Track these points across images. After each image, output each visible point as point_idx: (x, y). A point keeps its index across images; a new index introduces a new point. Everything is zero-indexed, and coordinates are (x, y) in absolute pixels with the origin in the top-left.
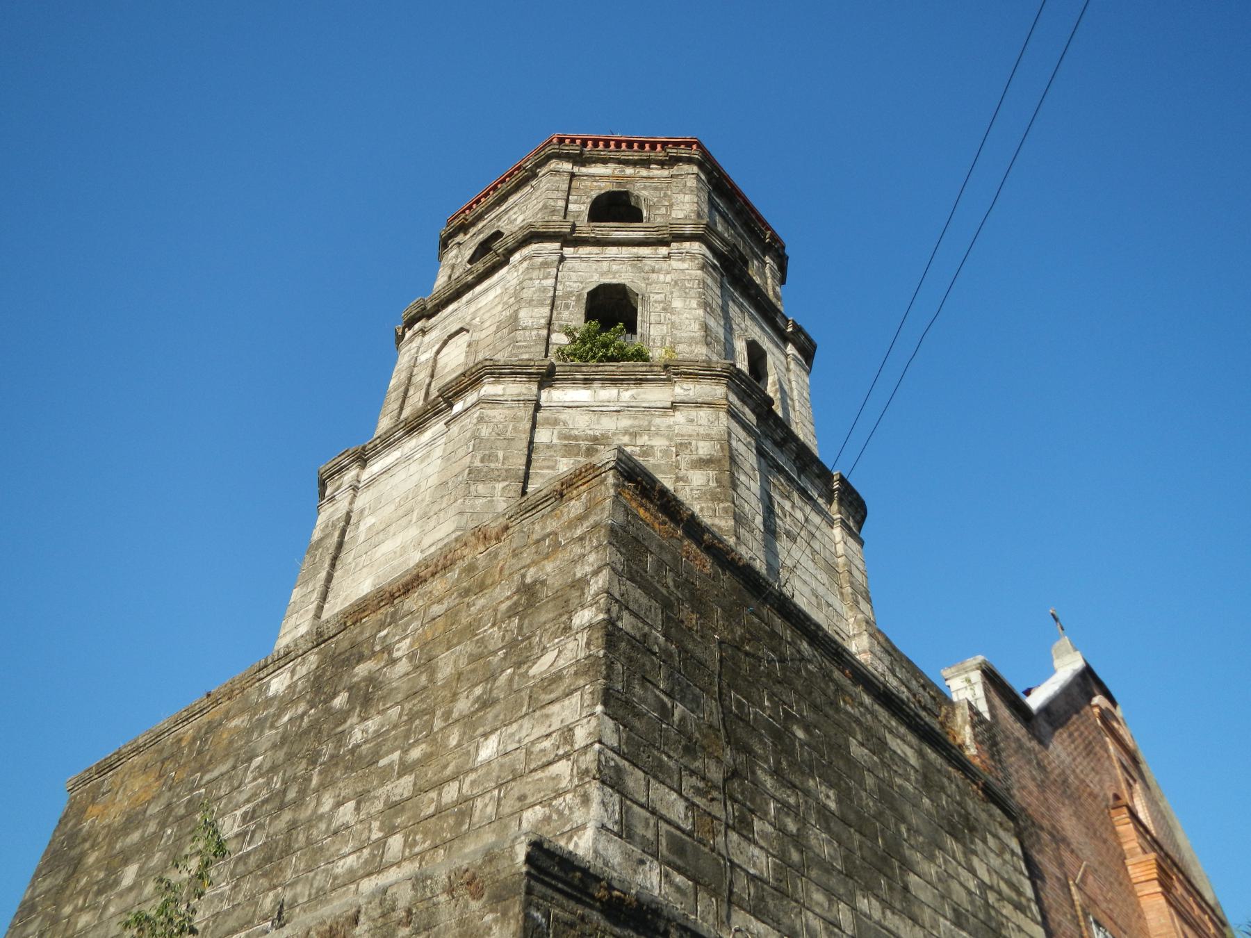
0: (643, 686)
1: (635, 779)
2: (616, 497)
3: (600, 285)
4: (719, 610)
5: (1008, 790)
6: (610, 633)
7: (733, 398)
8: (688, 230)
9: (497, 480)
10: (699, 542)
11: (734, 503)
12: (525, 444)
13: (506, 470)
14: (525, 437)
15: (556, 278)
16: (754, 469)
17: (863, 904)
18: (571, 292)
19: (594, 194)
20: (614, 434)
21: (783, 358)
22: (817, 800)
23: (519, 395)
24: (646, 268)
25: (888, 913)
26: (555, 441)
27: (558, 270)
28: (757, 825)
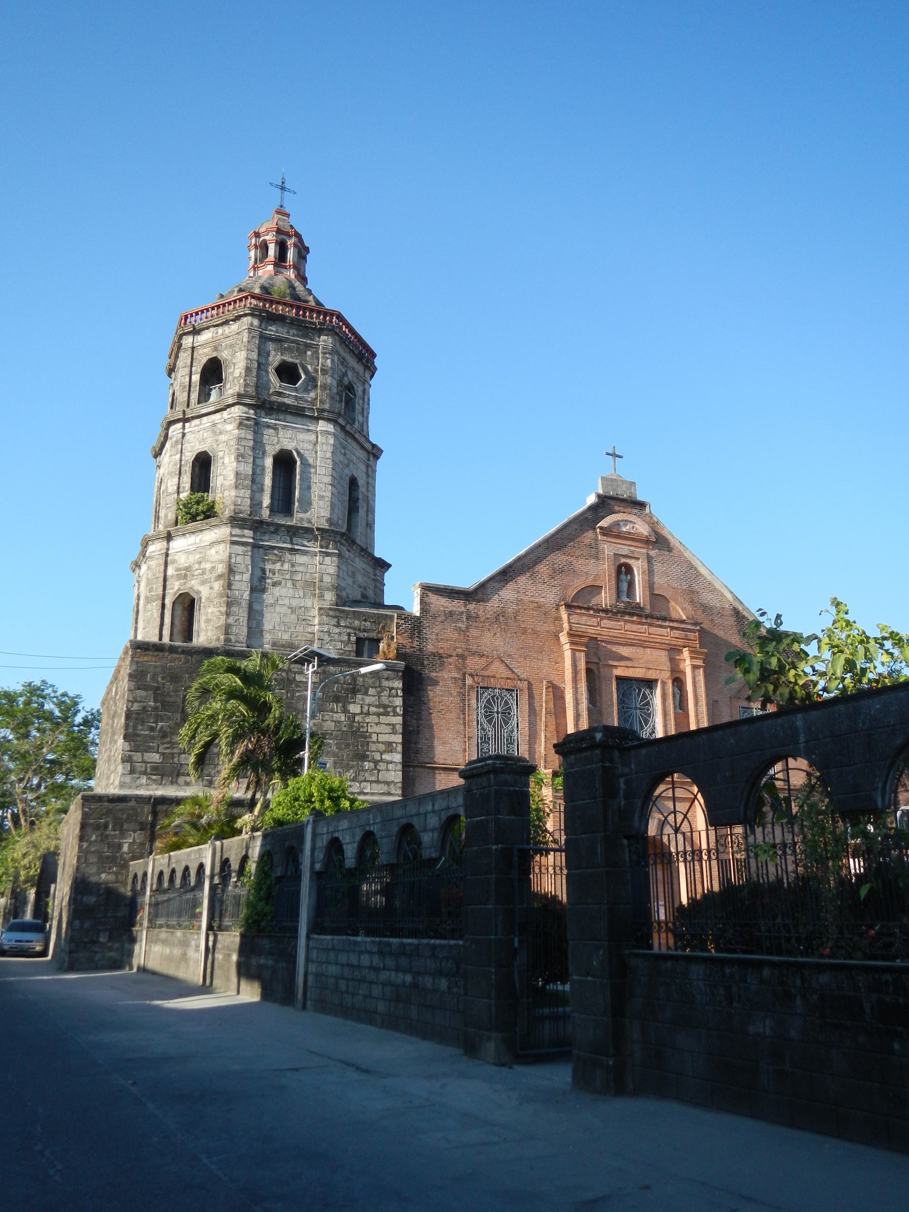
0: (142, 725)
1: (137, 756)
2: (132, 660)
3: (199, 453)
4: (187, 676)
5: (420, 650)
6: (128, 717)
7: (237, 531)
8: (230, 401)
10: (177, 653)
11: (228, 597)
12: (162, 579)
14: (162, 575)
19: (204, 361)
20: (194, 564)
21: (312, 437)
24: (218, 431)
27: (182, 445)
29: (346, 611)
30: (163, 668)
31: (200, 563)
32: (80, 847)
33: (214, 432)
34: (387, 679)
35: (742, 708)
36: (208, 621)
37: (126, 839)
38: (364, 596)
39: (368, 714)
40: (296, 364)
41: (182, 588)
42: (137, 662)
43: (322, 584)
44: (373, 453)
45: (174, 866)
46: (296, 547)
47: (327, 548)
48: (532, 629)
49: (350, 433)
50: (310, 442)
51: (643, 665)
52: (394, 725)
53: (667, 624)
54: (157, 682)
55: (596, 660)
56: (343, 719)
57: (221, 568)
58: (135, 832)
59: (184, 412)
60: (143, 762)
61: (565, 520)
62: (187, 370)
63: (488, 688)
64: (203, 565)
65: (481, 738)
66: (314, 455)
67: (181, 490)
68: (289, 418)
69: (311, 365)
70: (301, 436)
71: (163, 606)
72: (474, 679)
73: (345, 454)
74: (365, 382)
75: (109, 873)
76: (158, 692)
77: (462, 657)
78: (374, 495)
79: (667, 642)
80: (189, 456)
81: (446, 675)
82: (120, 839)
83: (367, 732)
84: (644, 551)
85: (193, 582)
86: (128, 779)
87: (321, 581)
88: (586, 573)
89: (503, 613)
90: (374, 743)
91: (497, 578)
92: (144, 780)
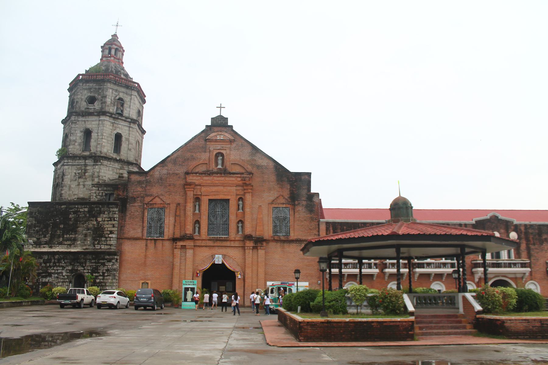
5: (127, 196)
17: (65, 236)
30: (38, 210)
34: (112, 208)
35: (274, 207)
38: (119, 177)
39: (104, 221)
42: (30, 209)
43: (95, 176)
48: (173, 184)
49: (116, 118)
50: (97, 124)
51: (222, 194)
52: (114, 224)
56: (95, 223)
57: (62, 175)
65: (149, 227)
68: (90, 117)
70: (93, 123)
76: (36, 219)
77: (143, 197)
81: (136, 204)
83: (104, 227)
84: (229, 146)
87: (94, 175)
89: (161, 179)
90: (106, 231)
91: (159, 166)
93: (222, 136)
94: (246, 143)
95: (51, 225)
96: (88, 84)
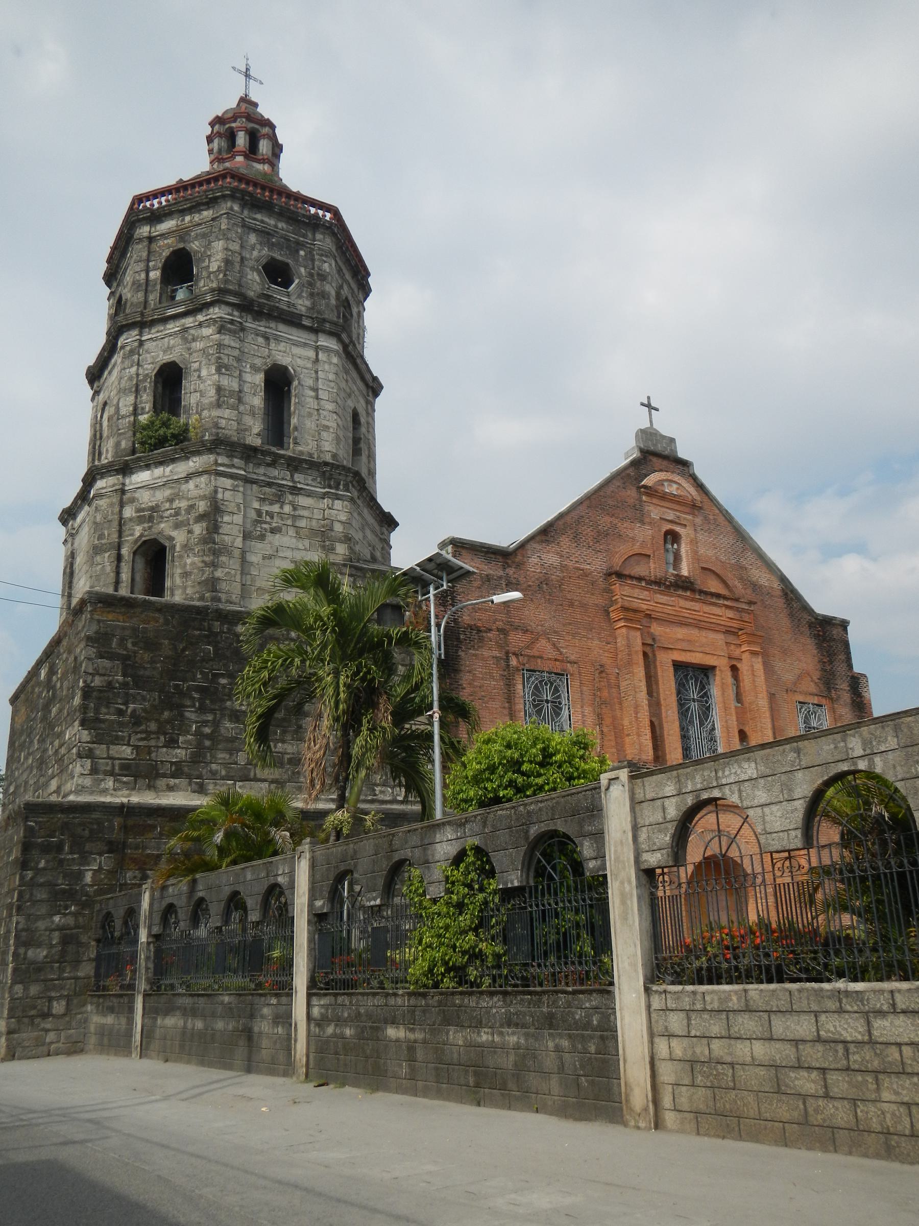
0: (108, 707)
1: (100, 750)
3: (164, 364)
4: (166, 642)
6: (87, 693)
8: (209, 298)
9: (106, 552)
13: (110, 544)
15: (138, 364)
16: (238, 505)
18: (147, 375)
19: (166, 253)
20: (162, 503)
22: (232, 710)
23: (114, 486)
24: (190, 337)
25: (280, 745)
26: (134, 515)
28: (181, 739)
29: (364, 568)
30: (135, 630)
31: (171, 501)
32: (22, 878)
33: (185, 340)
35: (800, 702)
36: (186, 575)
37: (88, 865)
40: (287, 264)
41: (146, 533)
42: (99, 621)
43: (333, 534)
44: (372, 388)
45: (200, 894)
46: (299, 486)
47: (337, 488)
49: (352, 357)
50: (309, 359)
53: (721, 602)
54: (126, 649)
55: (650, 642)
57: (202, 506)
58: (101, 854)
59: (142, 314)
60: (109, 758)
61: (607, 475)
62: (142, 265)
63: (535, 671)
64: (176, 504)
66: (314, 375)
67: (139, 411)
68: (281, 327)
69: (305, 267)
70: (297, 351)
71: (119, 558)
72: (518, 658)
73: (347, 381)
74: (360, 304)
75: (65, 915)
76: (128, 663)
78: (375, 439)
79: (722, 623)
80: (150, 368)
81: (486, 653)
82: (81, 865)
84: (690, 517)
85: (162, 525)
86: (88, 781)
87: (332, 530)
88: (633, 539)
91: (538, 538)
92: (110, 783)
93: (675, 486)
94: (721, 519)
95: (196, 696)
96: (259, 216)
